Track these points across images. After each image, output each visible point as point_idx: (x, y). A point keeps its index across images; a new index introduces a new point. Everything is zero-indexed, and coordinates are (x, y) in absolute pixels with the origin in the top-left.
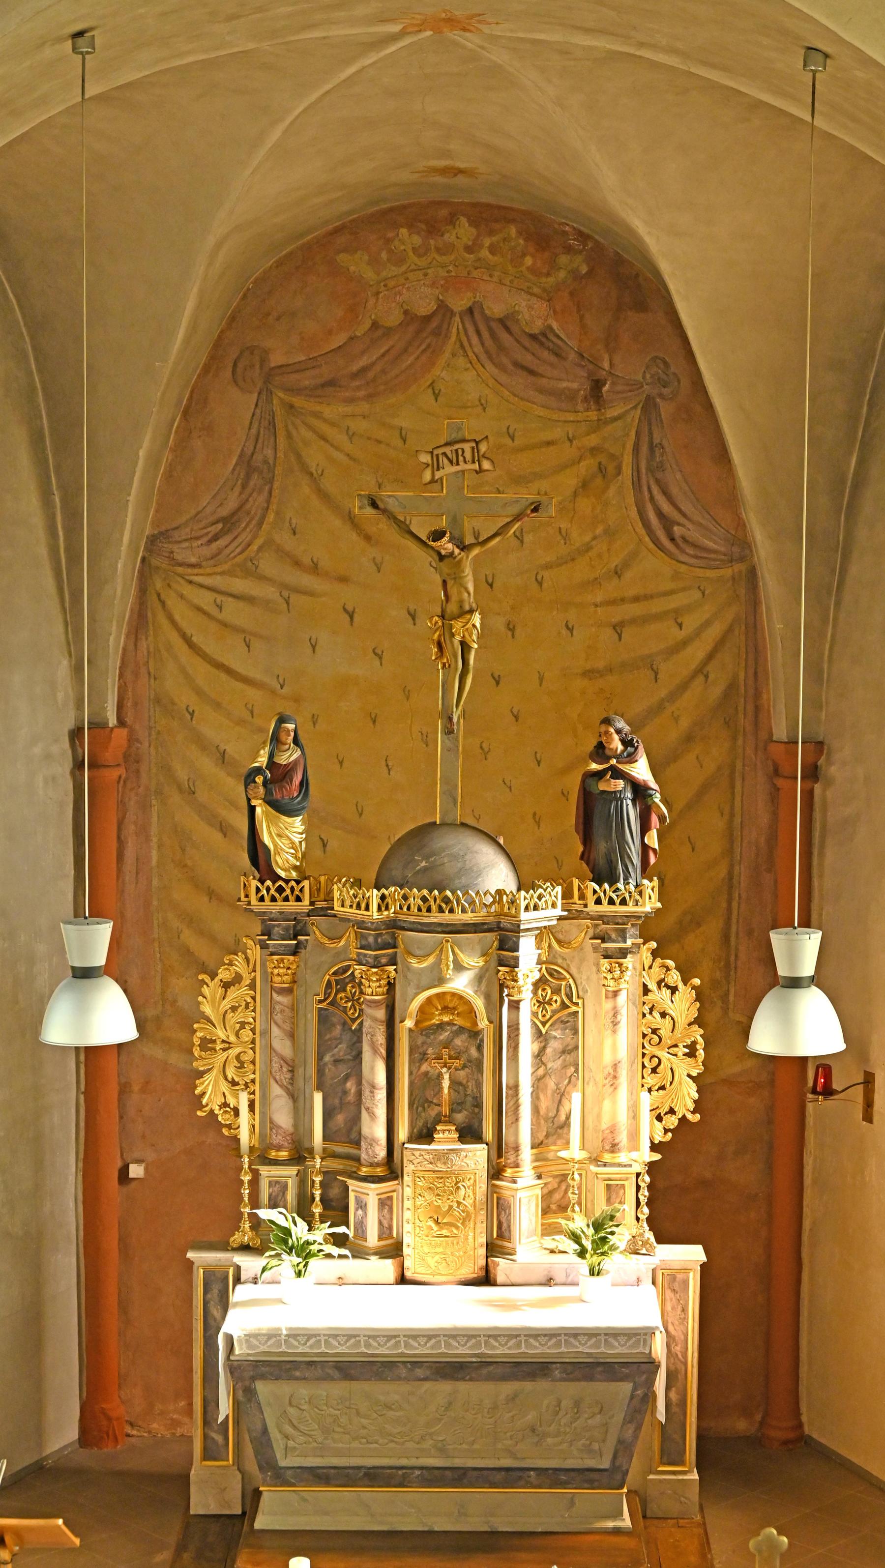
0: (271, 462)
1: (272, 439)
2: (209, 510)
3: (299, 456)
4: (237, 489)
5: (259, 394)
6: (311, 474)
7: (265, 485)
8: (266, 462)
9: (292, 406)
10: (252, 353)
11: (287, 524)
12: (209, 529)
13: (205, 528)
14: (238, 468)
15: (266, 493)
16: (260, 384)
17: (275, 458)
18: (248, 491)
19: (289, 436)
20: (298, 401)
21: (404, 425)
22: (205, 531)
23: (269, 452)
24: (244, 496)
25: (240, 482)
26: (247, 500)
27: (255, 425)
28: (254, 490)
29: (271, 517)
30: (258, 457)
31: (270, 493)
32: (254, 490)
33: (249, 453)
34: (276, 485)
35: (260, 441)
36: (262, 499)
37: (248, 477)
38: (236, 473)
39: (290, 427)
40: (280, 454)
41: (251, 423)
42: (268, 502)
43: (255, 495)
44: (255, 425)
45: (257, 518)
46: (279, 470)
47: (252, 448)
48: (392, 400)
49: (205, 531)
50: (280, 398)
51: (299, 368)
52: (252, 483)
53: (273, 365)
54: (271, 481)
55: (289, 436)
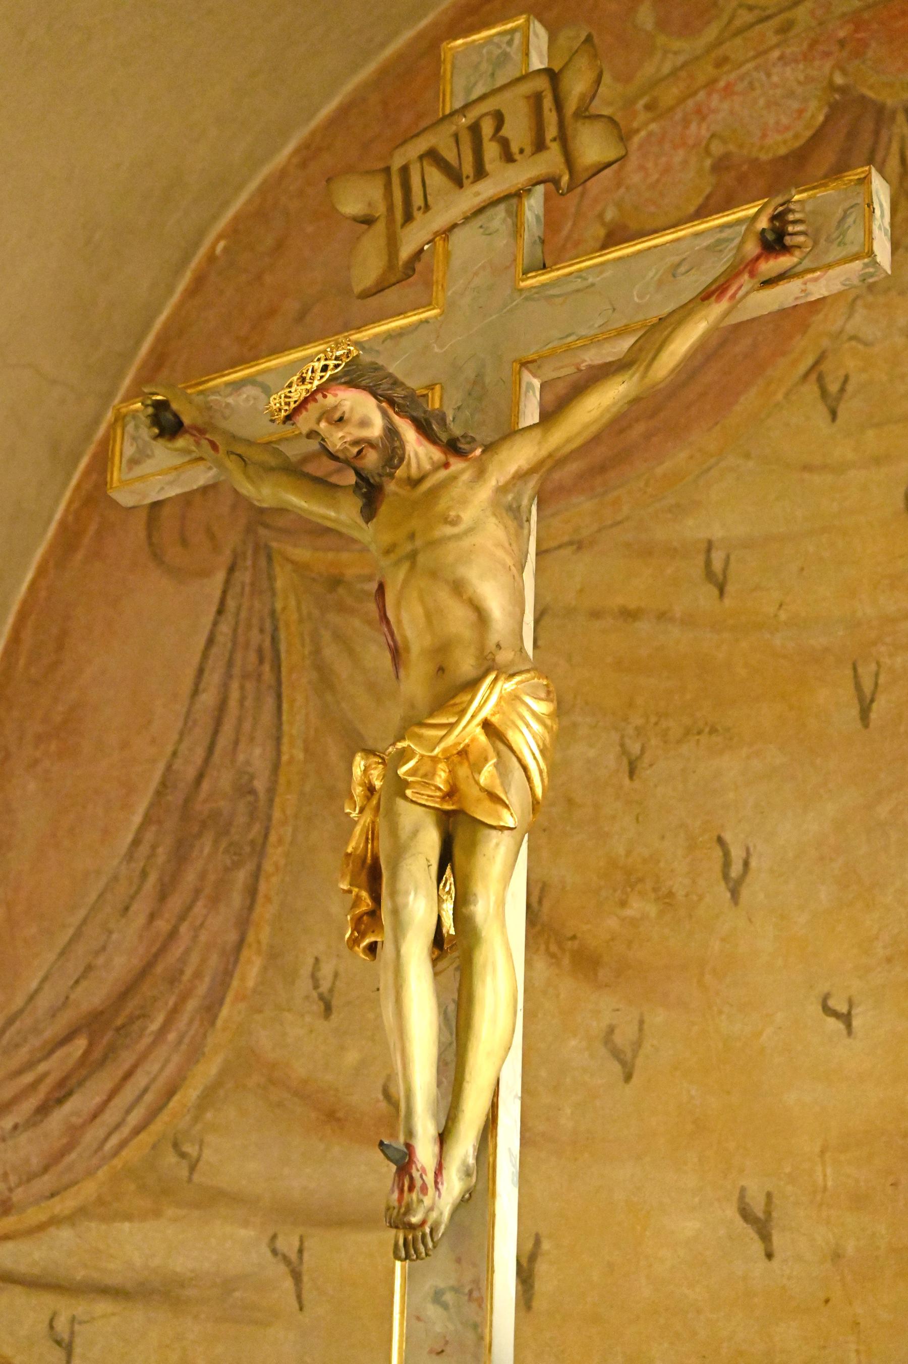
0: (260, 785)
1: (269, 702)
2: (44, 1002)
4: (141, 909)
5: (231, 570)
7: (236, 865)
11: (304, 984)
12: (42, 1068)
13: (30, 1065)
14: (149, 836)
15: (237, 899)
16: (231, 539)
17: (276, 767)
18: (176, 903)
21: (717, 532)
22: (28, 1078)
23: (257, 757)
24: (163, 925)
25: (152, 878)
26: (173, 934)
27: (213, 678)
28: (197, 892)
29: (251, 970)
30: (222, 779)
31: (252, 892)
33: (191, 773)
34: (275, 855)
35: (228, 727)
36: (219, 924)
37: (181, 855)
38: (144, 849)
39: (330, 651)
40: (293, 752)
41: (201, 671)
42: (244, 923)
43: (199, 908)
44: (213, 678)
45: (202, 988)
46: (287, 802)
47: (200, 753)
48: (678, 458)
49: (28, 1078)
50: (299, 567)
52: (190, 877)
54: (260, 849)
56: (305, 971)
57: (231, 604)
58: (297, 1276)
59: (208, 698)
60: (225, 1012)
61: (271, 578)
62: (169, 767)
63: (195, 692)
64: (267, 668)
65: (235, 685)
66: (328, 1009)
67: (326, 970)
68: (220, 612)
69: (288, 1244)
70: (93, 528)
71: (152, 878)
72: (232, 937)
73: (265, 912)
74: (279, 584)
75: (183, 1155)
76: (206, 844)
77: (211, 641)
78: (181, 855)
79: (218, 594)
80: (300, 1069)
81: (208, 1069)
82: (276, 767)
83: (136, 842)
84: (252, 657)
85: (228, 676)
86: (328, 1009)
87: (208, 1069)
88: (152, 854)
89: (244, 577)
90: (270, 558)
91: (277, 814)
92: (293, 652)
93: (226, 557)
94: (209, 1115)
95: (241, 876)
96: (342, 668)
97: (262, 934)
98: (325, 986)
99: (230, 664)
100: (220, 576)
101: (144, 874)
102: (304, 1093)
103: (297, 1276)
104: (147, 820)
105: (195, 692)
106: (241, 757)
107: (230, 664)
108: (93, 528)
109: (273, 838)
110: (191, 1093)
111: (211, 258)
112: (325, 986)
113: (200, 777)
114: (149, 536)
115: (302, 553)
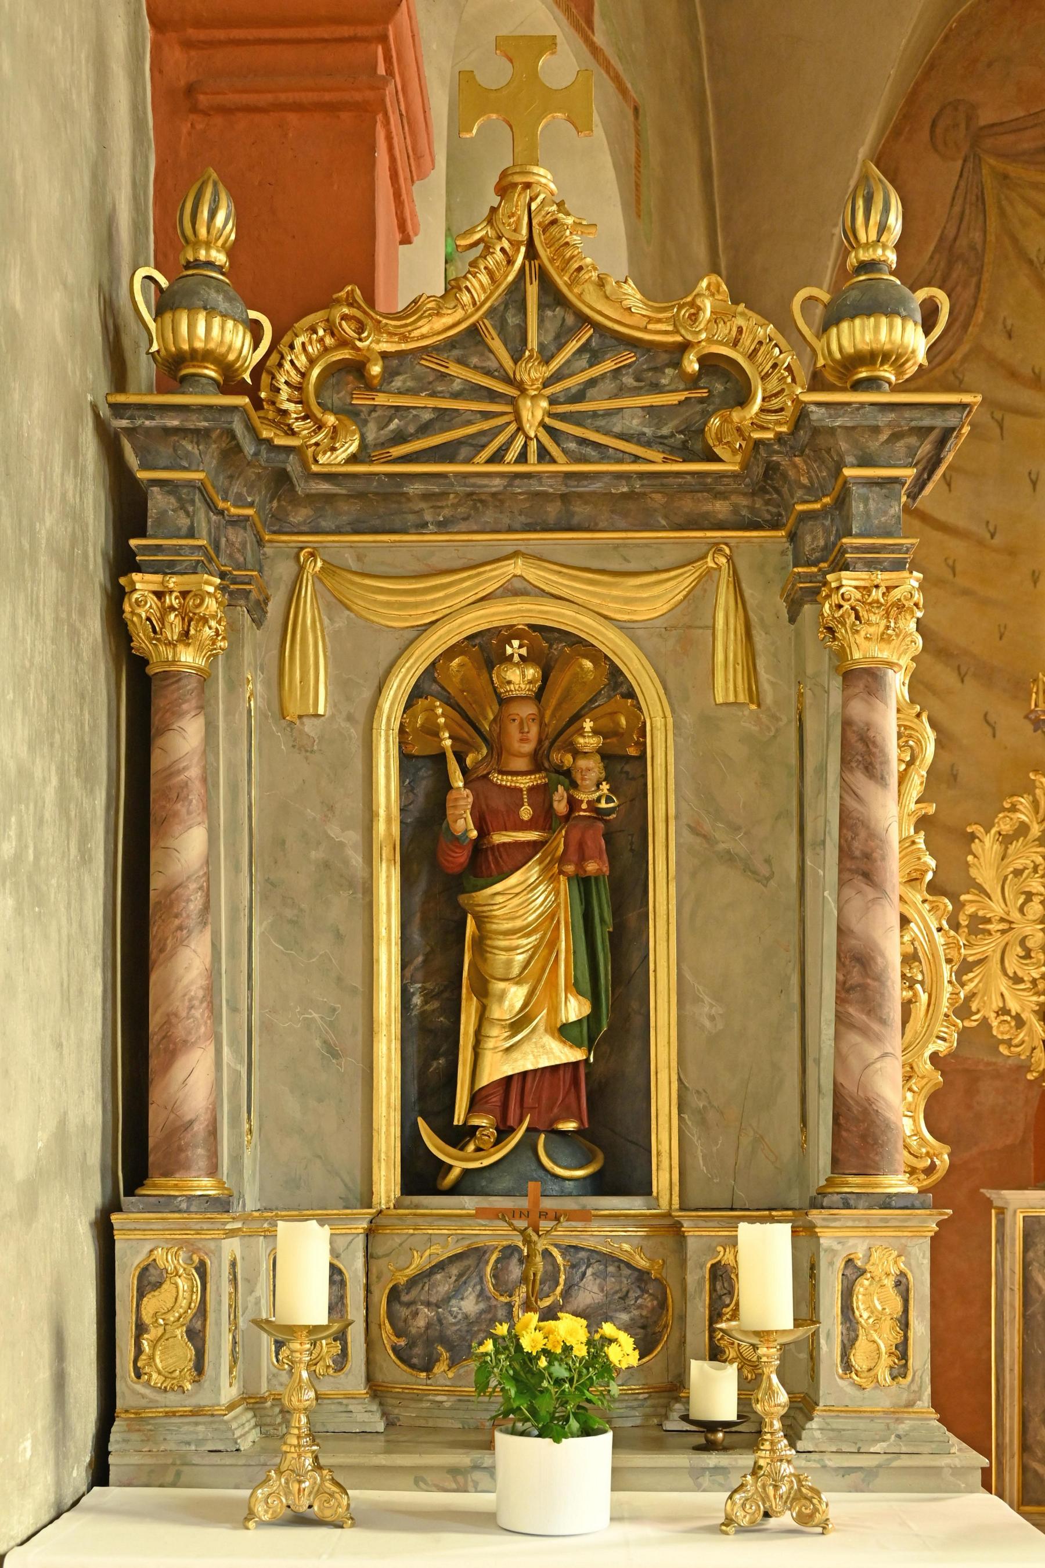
0: (979, 247)
1: (981, 217)
3: (1014, 240)
5: (965, 161)
6: (1031, 262)
8: (972, 247)
9: (1006, 177)
10: (956, 109)
11: (1000, 326)
14: (937, 256)
17: (985, 242)
19: (1002, 214)
20: (1014, 170)
23: (977, 236)
25: (939, 274)
27: (959, 201)
29: (980, 316)
30: (963, 242)
31: (978, 286)
32: (957, 283)
34: (986, 276)
37: (950, 266)
38: (935, 261)
40: (991, 238)
41: (954, 198)
42: (976, 298)
44: (959, 201)
46: (989, 257)
51: (1017, 127)
52: (954, 275)
53: (982, 122)
54: (980, 271)
55: (1002, 214)
56: (1001, 320)
57: (965, 174)
58: (1002, 428)
59: (957, 209)
60: (970, 329)
61: (981, 169)
62: (943, 232)
63: (952, 205)
64: (980, 203)
65: (967, 206)
66: (1010, 337)
67: (1009, 322)
68: (961, 176)
69: (998, 415)
70: (907, 129)
71: (939, 274)
72: (972, 302)
73: (984, 296)
74: (984, 171)
75: (957, 377)
76: (959, 266)
77: (957, 188)
78: (950, 266)
79: (959, 169)
80: (1001, 355)
81: (965, 348)
82: (985, 242)
83: (932, 258)
84: (974, 198)
85: (964, 203)
86: (1010, 337)
87: (965, 348)
88: (938, 264)
89: (970, 165)
90: (980, 160)
91: (986, 260)
92: (989, 200)
93: (963, 154)
94: (966, 365)
95: (974, 280)
96: (1009, 210)
97: (983, 303)
98: (1009, 328)
99: (965, 198)
100: (960, 163)
101: (936, 271)
102: (1001, 364)
103: (1002, 428)
104: (934, 252)
105: (952, 205)
106: (971, 235)
107: (965, 198)
108: (907, 129)
109: (985, 269)
110: (958, 356)
111: (951, 30)
112: (1009, 328)
113: (955, 239)
114: (931, 138)
115: (992, 161)
